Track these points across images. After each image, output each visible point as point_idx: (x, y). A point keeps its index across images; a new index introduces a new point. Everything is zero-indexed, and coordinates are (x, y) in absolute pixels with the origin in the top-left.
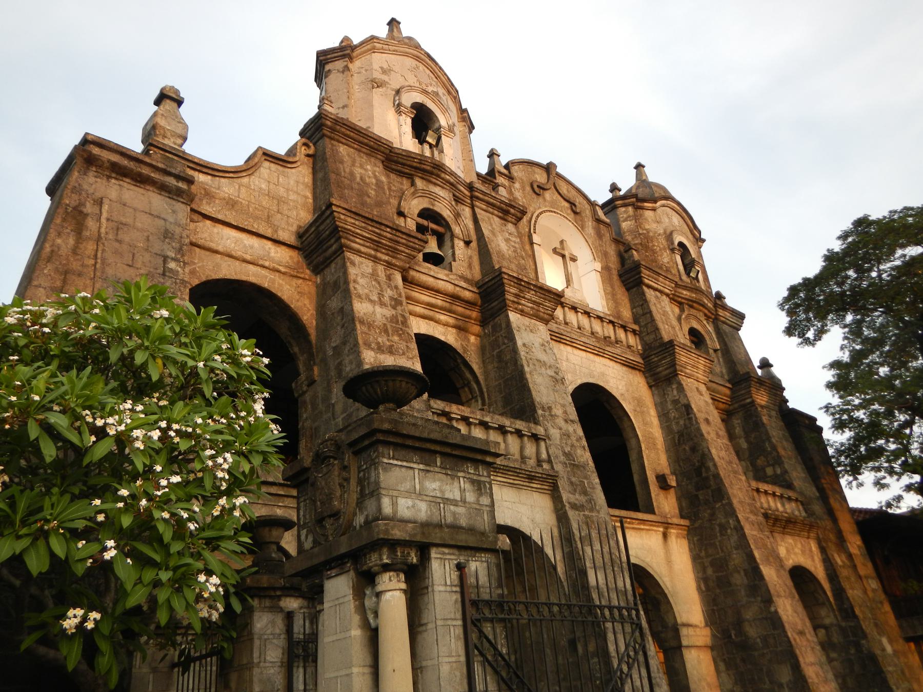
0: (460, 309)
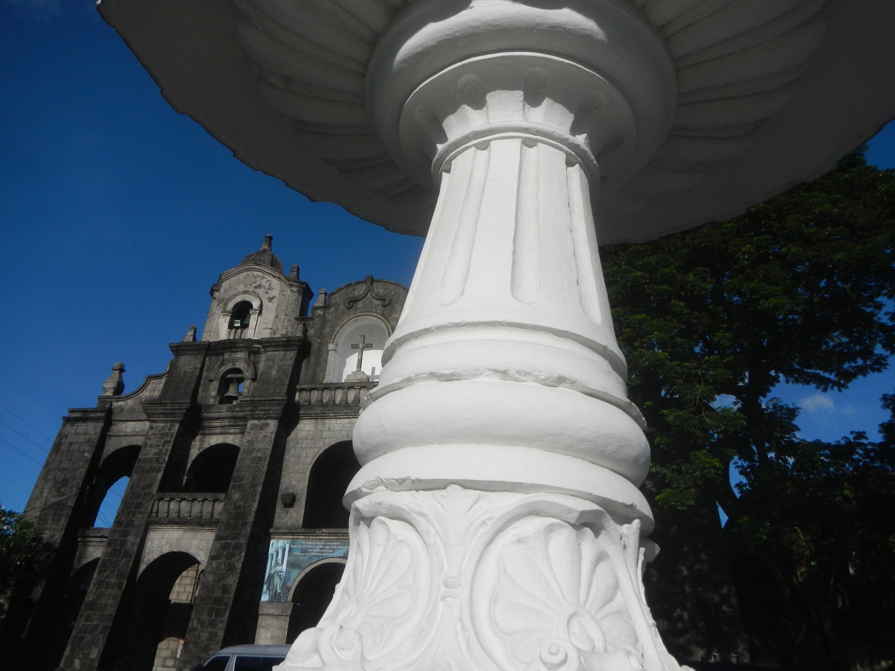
0: (241, 423)
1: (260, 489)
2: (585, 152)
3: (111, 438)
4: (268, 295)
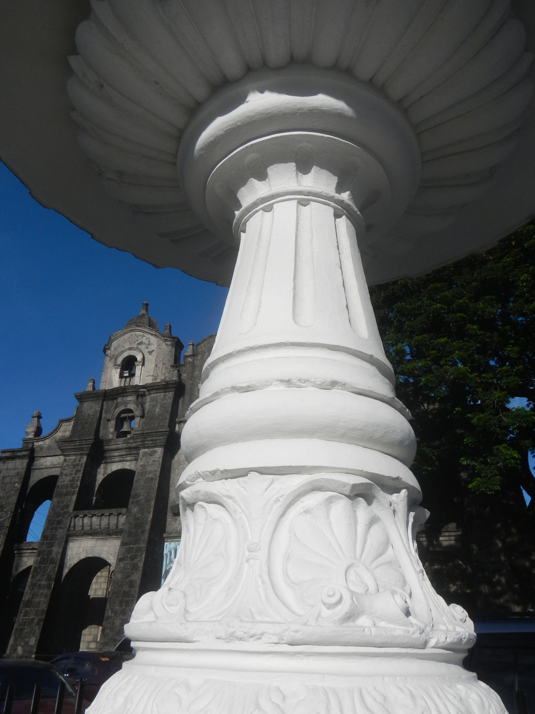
0: (135, 452)
1: (153, 503)
2: (349, 205)
3: (35, 471)
4: (148, 350)
